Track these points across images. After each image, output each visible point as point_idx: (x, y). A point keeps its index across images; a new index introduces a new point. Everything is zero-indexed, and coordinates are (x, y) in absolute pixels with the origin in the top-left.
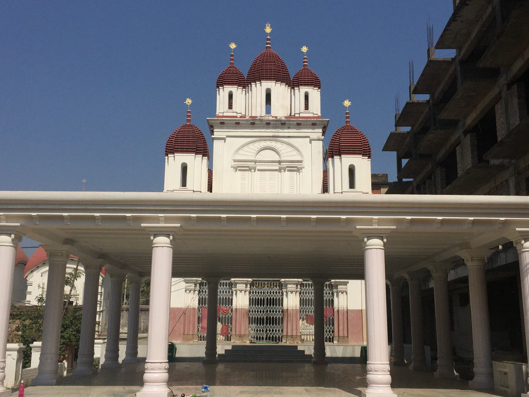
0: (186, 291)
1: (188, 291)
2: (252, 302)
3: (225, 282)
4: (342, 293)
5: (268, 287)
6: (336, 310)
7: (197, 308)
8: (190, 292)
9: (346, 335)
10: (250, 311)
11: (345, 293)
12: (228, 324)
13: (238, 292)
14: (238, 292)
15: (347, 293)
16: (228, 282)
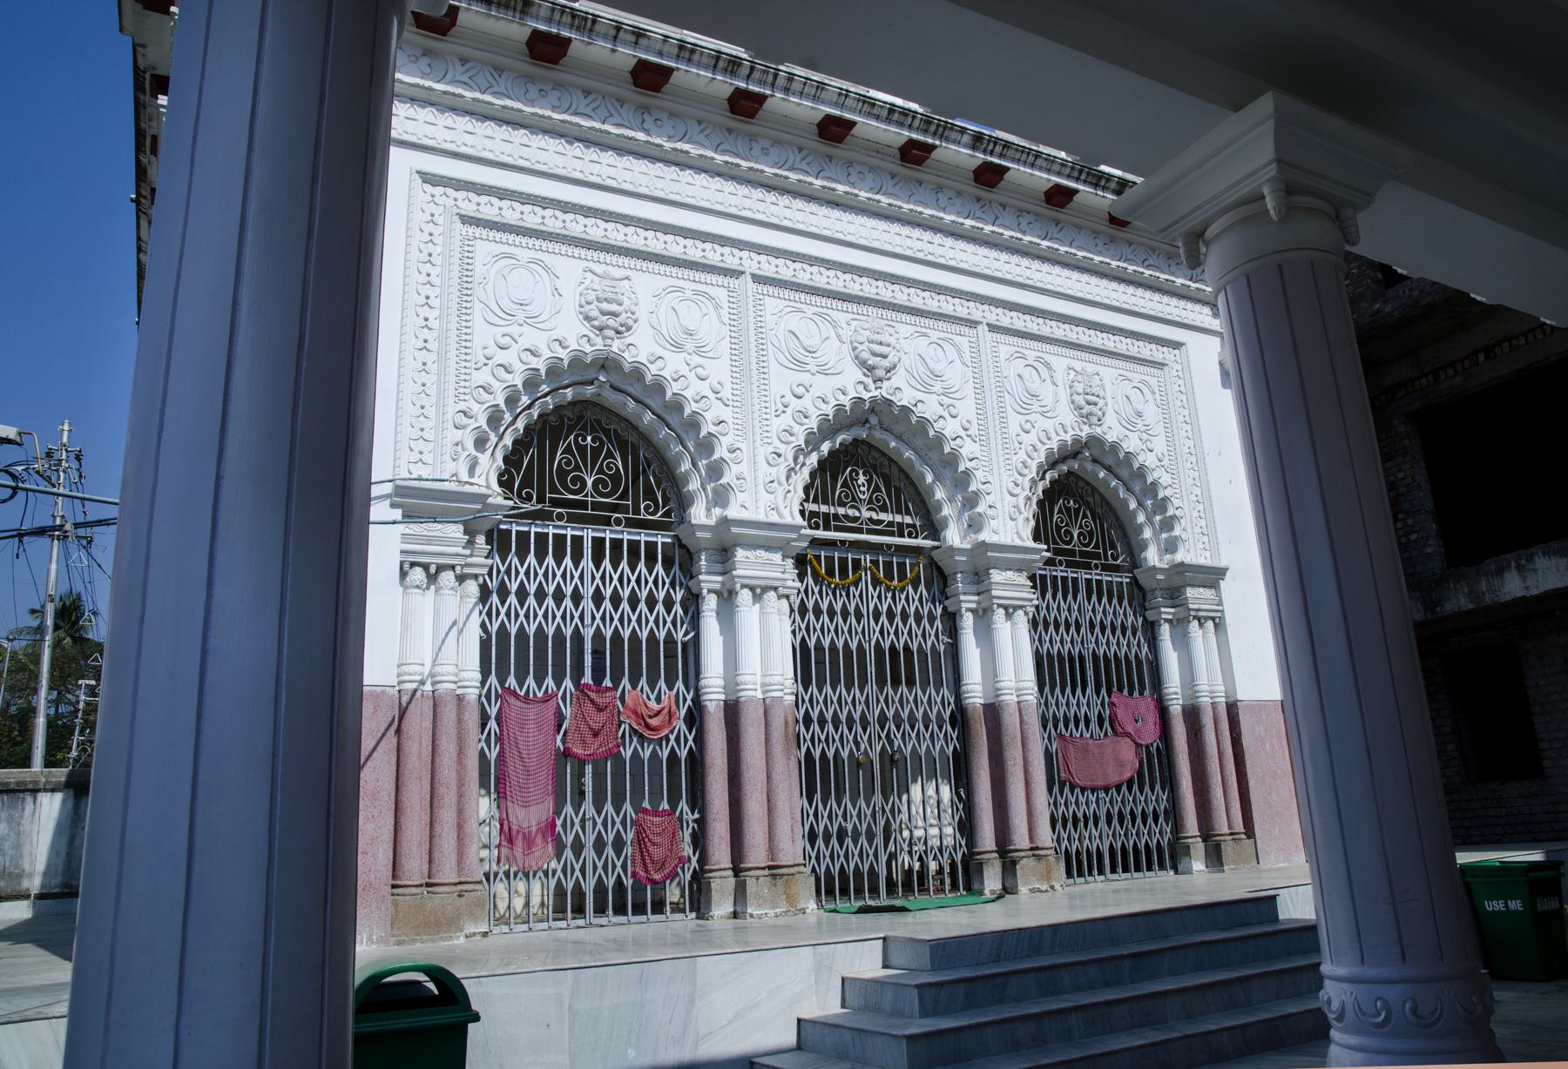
0: (403, 574)
1: (418, 575)
2: (810, 663)
3: (643, 537)
4: (1201, 621)
5: (876, 582)
6: (1176, 709)
7: (472, 693)
8: (432, 578)
9: (1239, 825)
10: (807, 720)
11: (1210, 623)
12: (674, 803)
13: (745, 596)
14: (745, 596)
15: (1219, 624)
16: (661, 539)
